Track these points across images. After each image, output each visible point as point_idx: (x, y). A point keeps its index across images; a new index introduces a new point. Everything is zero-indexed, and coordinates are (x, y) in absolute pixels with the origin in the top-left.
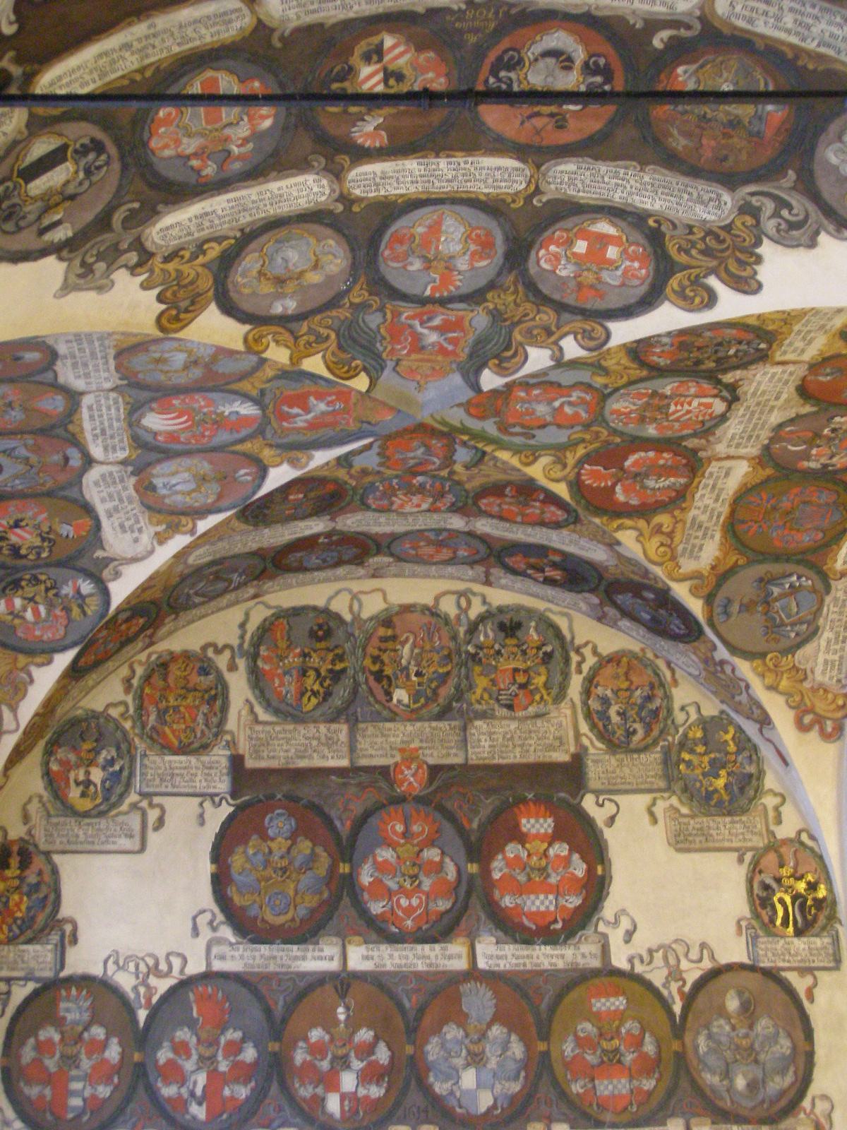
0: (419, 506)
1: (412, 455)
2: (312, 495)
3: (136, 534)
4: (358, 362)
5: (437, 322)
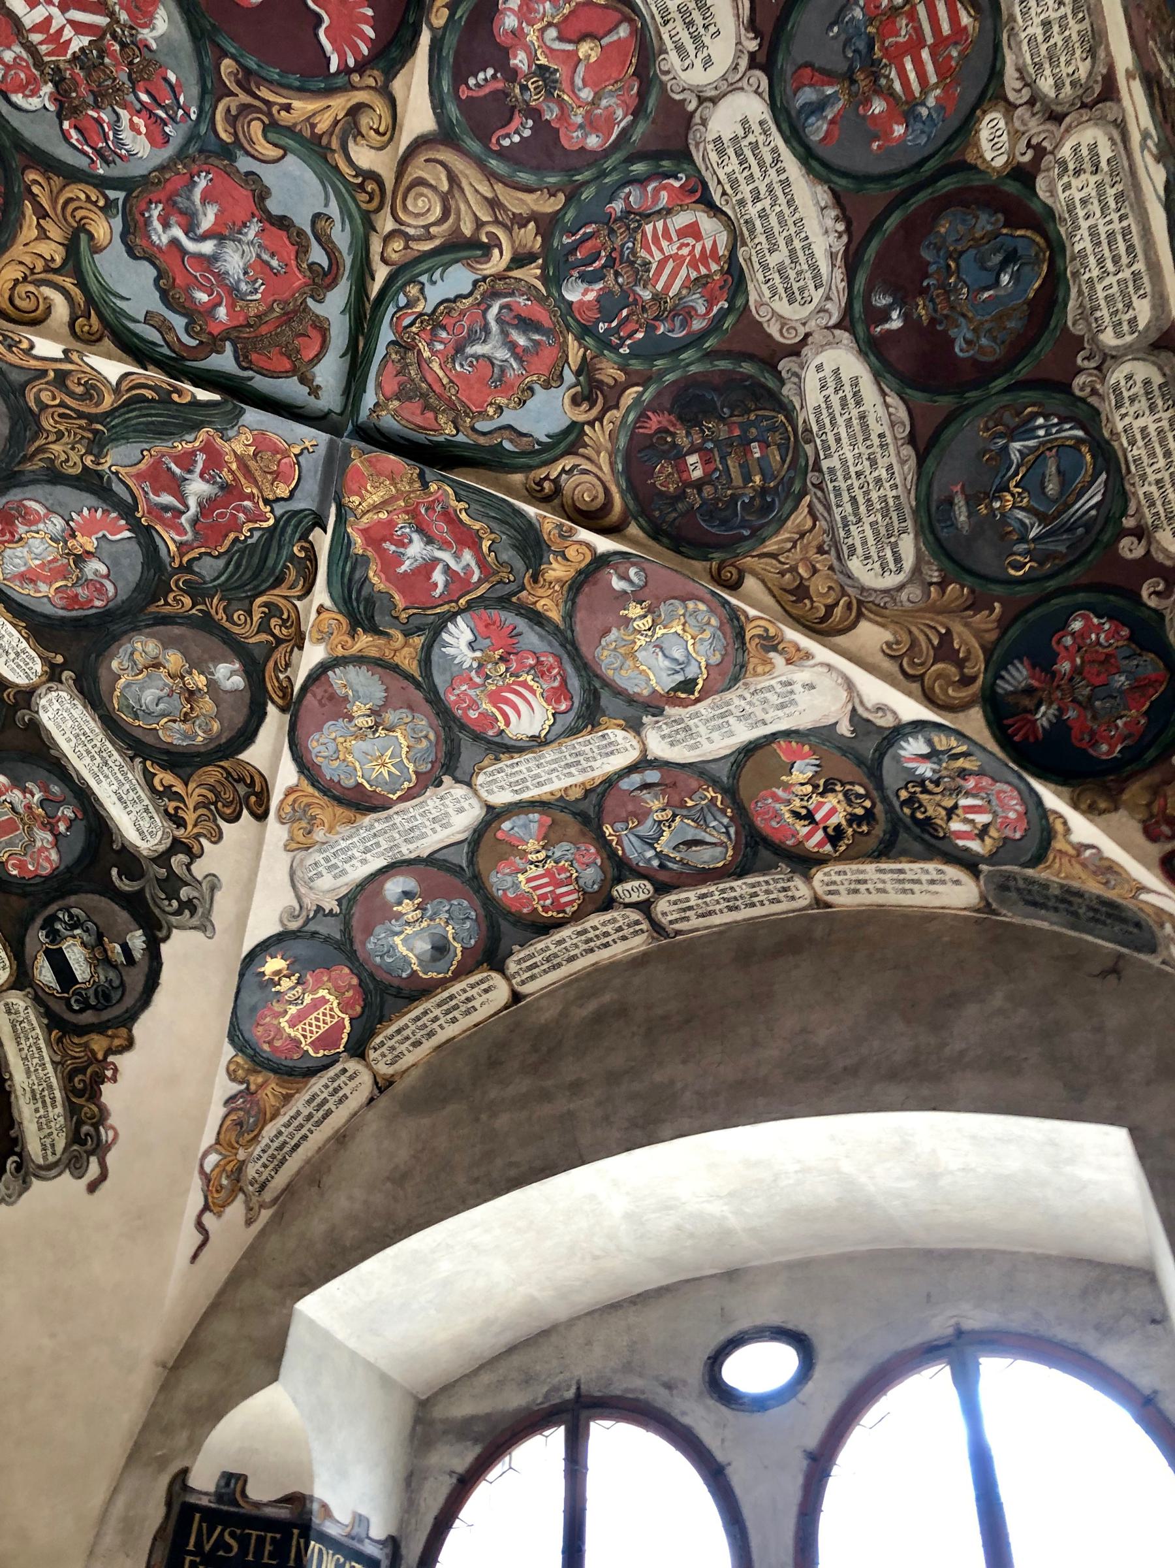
0: (693, 231)
1: (502, 354)
2: (683, 440)
3: (797, 688)
4: (295, 550)
5: (166, 499)
